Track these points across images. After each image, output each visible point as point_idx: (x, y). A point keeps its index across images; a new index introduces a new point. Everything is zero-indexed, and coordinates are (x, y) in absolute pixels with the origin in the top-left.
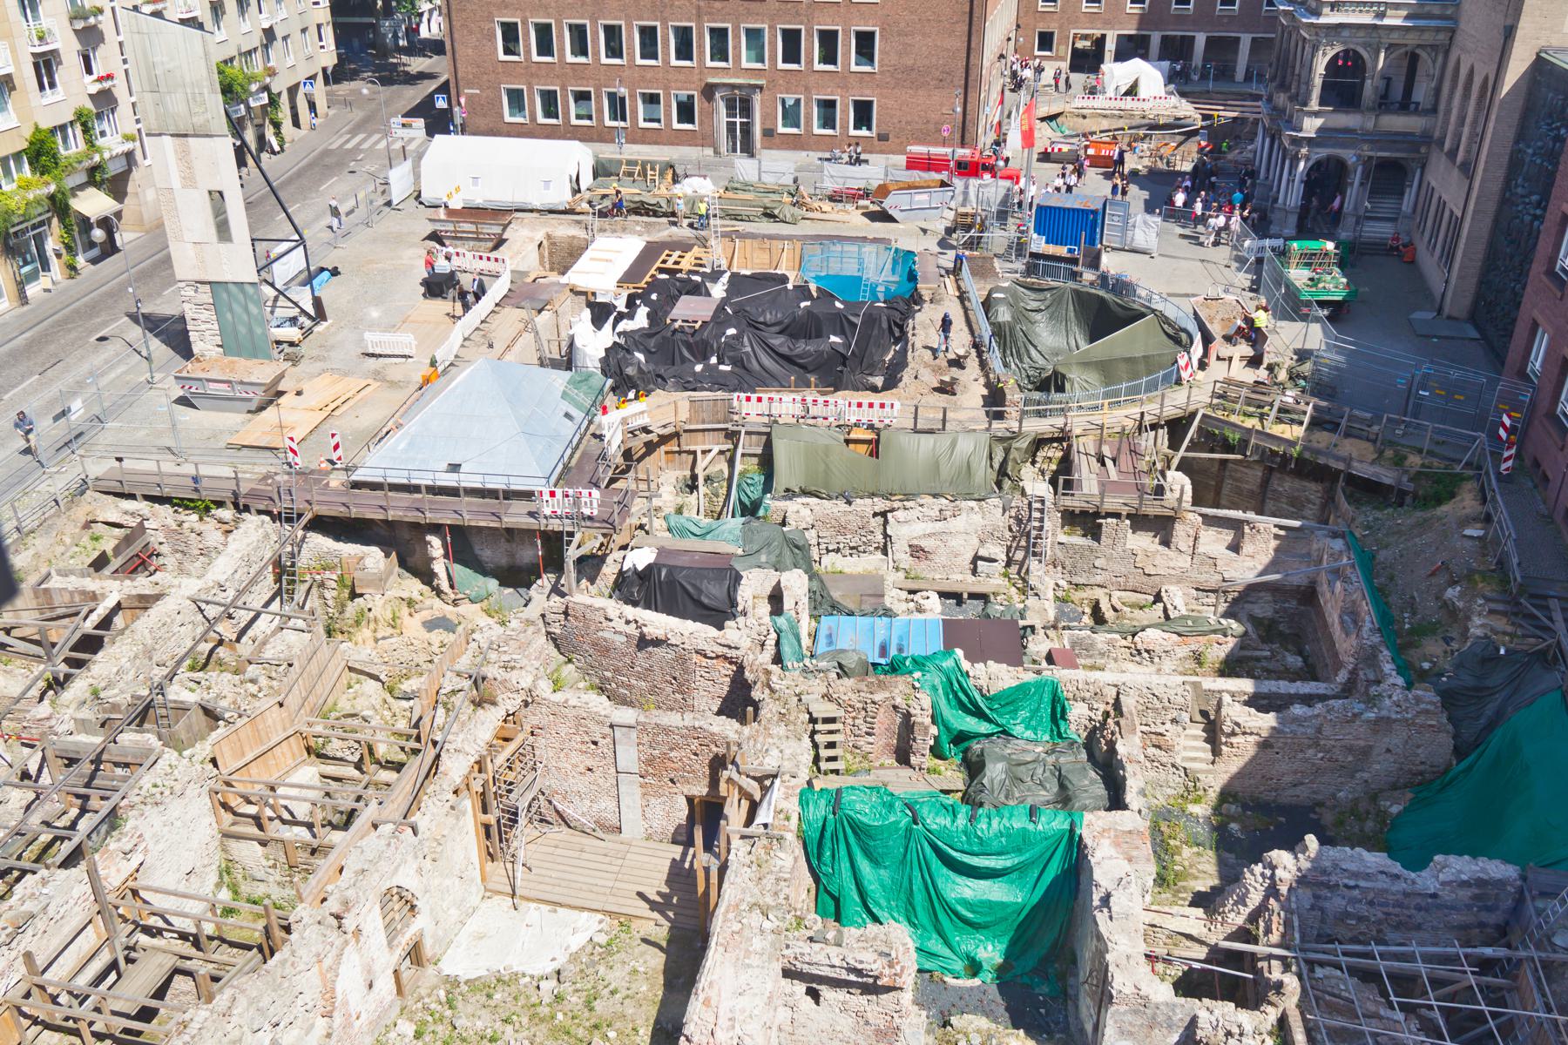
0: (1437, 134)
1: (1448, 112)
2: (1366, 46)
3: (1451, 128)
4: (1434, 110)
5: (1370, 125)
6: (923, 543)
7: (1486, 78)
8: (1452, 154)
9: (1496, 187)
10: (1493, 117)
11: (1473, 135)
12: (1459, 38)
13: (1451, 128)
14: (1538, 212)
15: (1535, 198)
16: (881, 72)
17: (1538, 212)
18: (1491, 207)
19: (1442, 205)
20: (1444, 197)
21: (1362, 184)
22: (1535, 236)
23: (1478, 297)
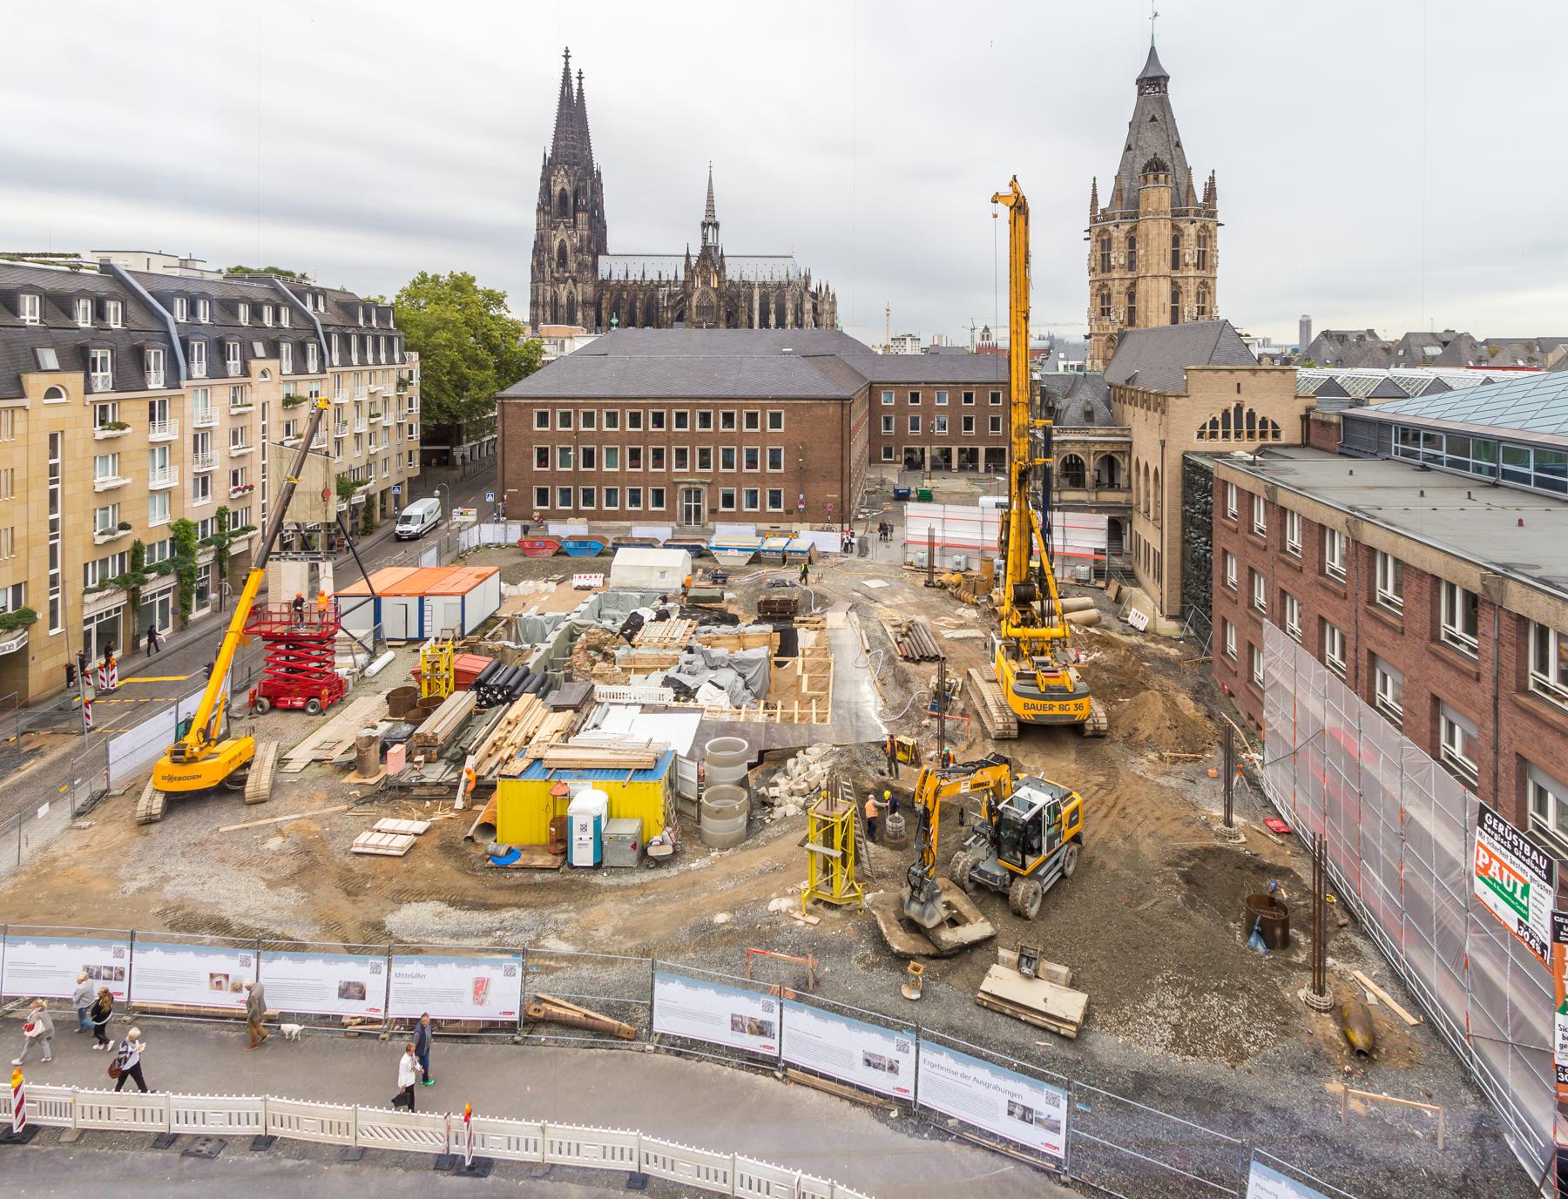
0: (1134, 502)
1: (1138, 489)
3: (1142, 498)
4: (1130, 487)
5: (1093, 497)
10: (1166, 491)
11: (1156, 502)
12: (1135, 446)
13: (1142, 498)
16: (786, 472)
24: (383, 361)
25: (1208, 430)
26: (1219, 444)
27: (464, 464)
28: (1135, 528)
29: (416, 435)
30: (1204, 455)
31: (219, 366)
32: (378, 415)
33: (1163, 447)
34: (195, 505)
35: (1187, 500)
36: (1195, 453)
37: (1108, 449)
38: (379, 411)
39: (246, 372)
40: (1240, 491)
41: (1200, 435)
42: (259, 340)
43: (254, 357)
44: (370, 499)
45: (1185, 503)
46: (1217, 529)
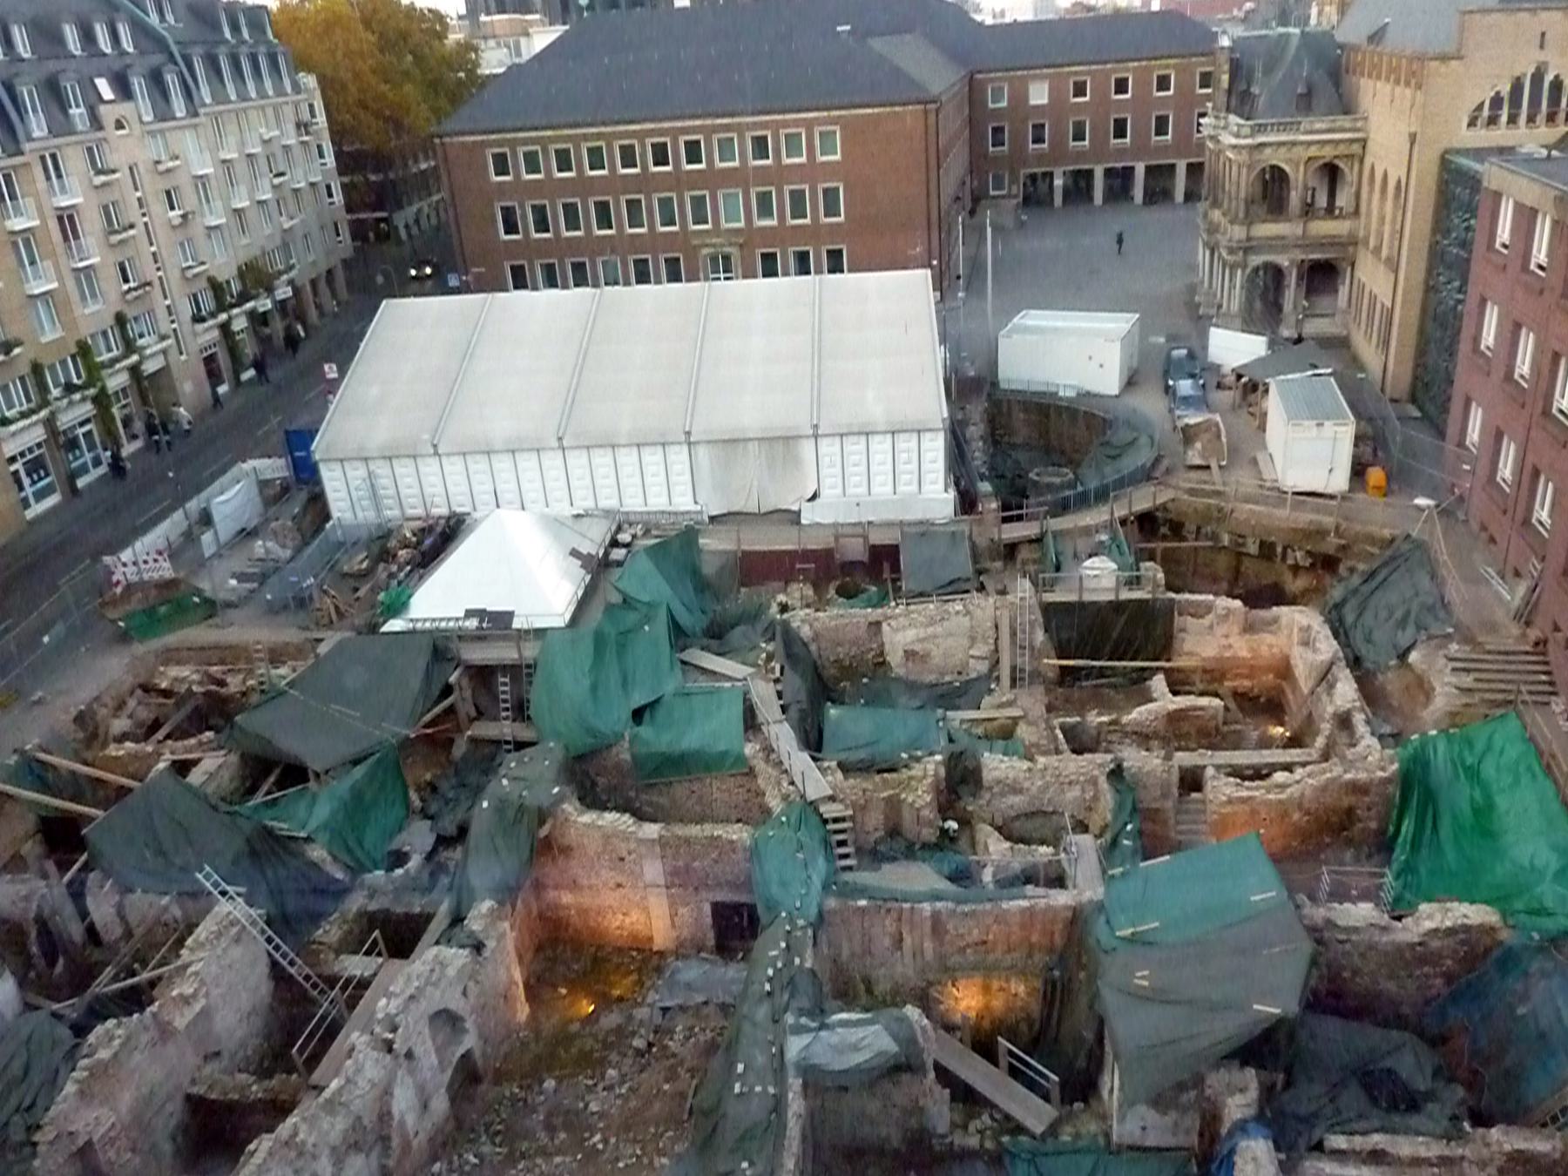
0: (1361, 234)
2: (1289, 161)
3: (1374, 226)
4: (1357, 212)
6: (917, 647)
7: (1399, 182)
8: (1377, 251)
9: (1420, 276)
10: (1409, 215)
11: (1393, 232)
12: (1370, 144)
13: (1374, 226)
14: (1461, 296)
15: (1457, 284)
17: (1461, 296)
18: (1418, 295)
19: (1373, 299)
20: (1375, 290)
21: (1298, 285)
22: (1459, 317)
23: (1415, 378)
24: (271, 93)
25: (1486, 112)
26: (1501, 135)
27: (410, 235)
28: (1359, 274)
29: (338, 198)
30: (1479, 154)
31: (60, 117)
32: (282, 174)
33: (1412, 143)
34: (87, 311)
35: (1440, 226)
36: (1458, 152)
37: (1328, 153)
38: (281, 169)
39: (96, 123)
40: (1519, 207)
41: (1472, 123)
42: (100, 75)
43: (101, 100)
44: (297, 291)
45: (1435, 231)
46: (1476, 268)
